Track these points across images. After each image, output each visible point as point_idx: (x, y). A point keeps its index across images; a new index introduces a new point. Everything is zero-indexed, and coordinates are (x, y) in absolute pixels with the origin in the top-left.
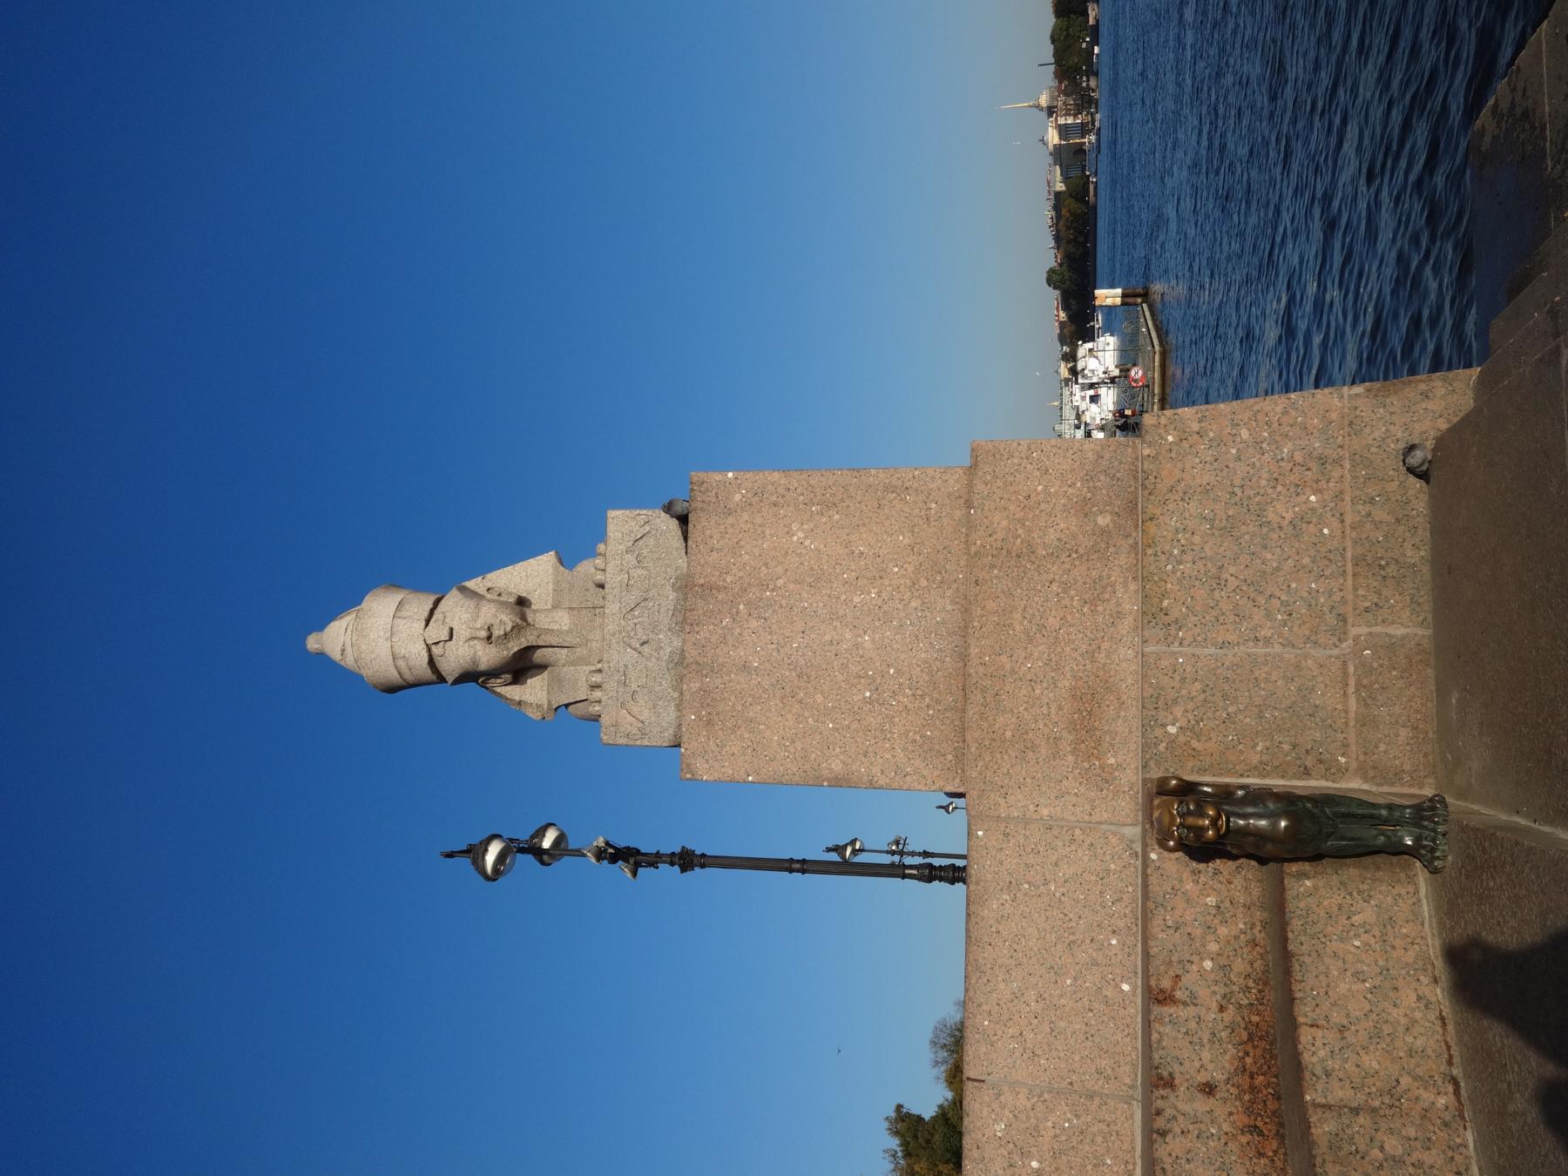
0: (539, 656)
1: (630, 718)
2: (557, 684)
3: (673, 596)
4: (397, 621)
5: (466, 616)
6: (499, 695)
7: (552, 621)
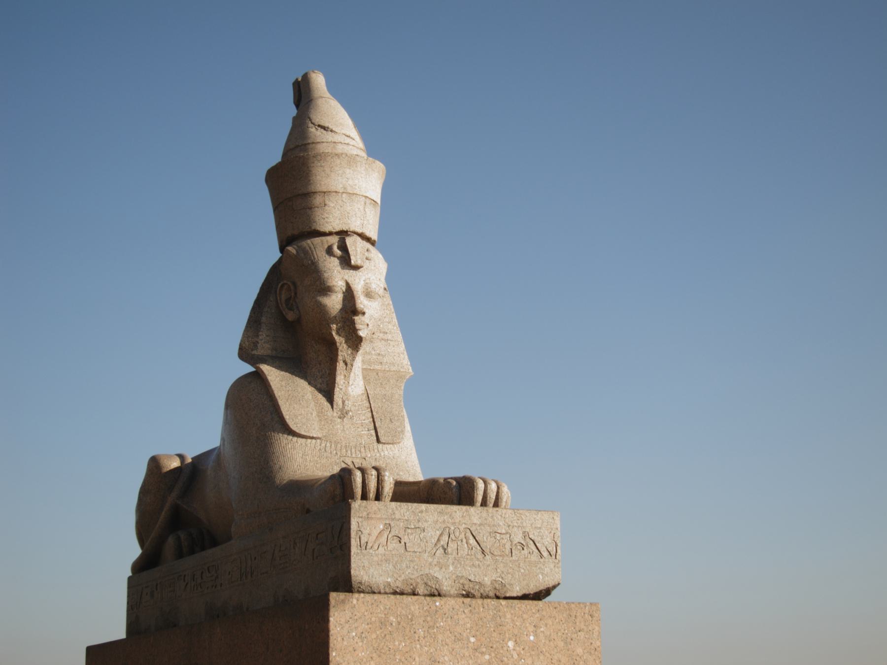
1: (375, 533)
3: (487, 581)
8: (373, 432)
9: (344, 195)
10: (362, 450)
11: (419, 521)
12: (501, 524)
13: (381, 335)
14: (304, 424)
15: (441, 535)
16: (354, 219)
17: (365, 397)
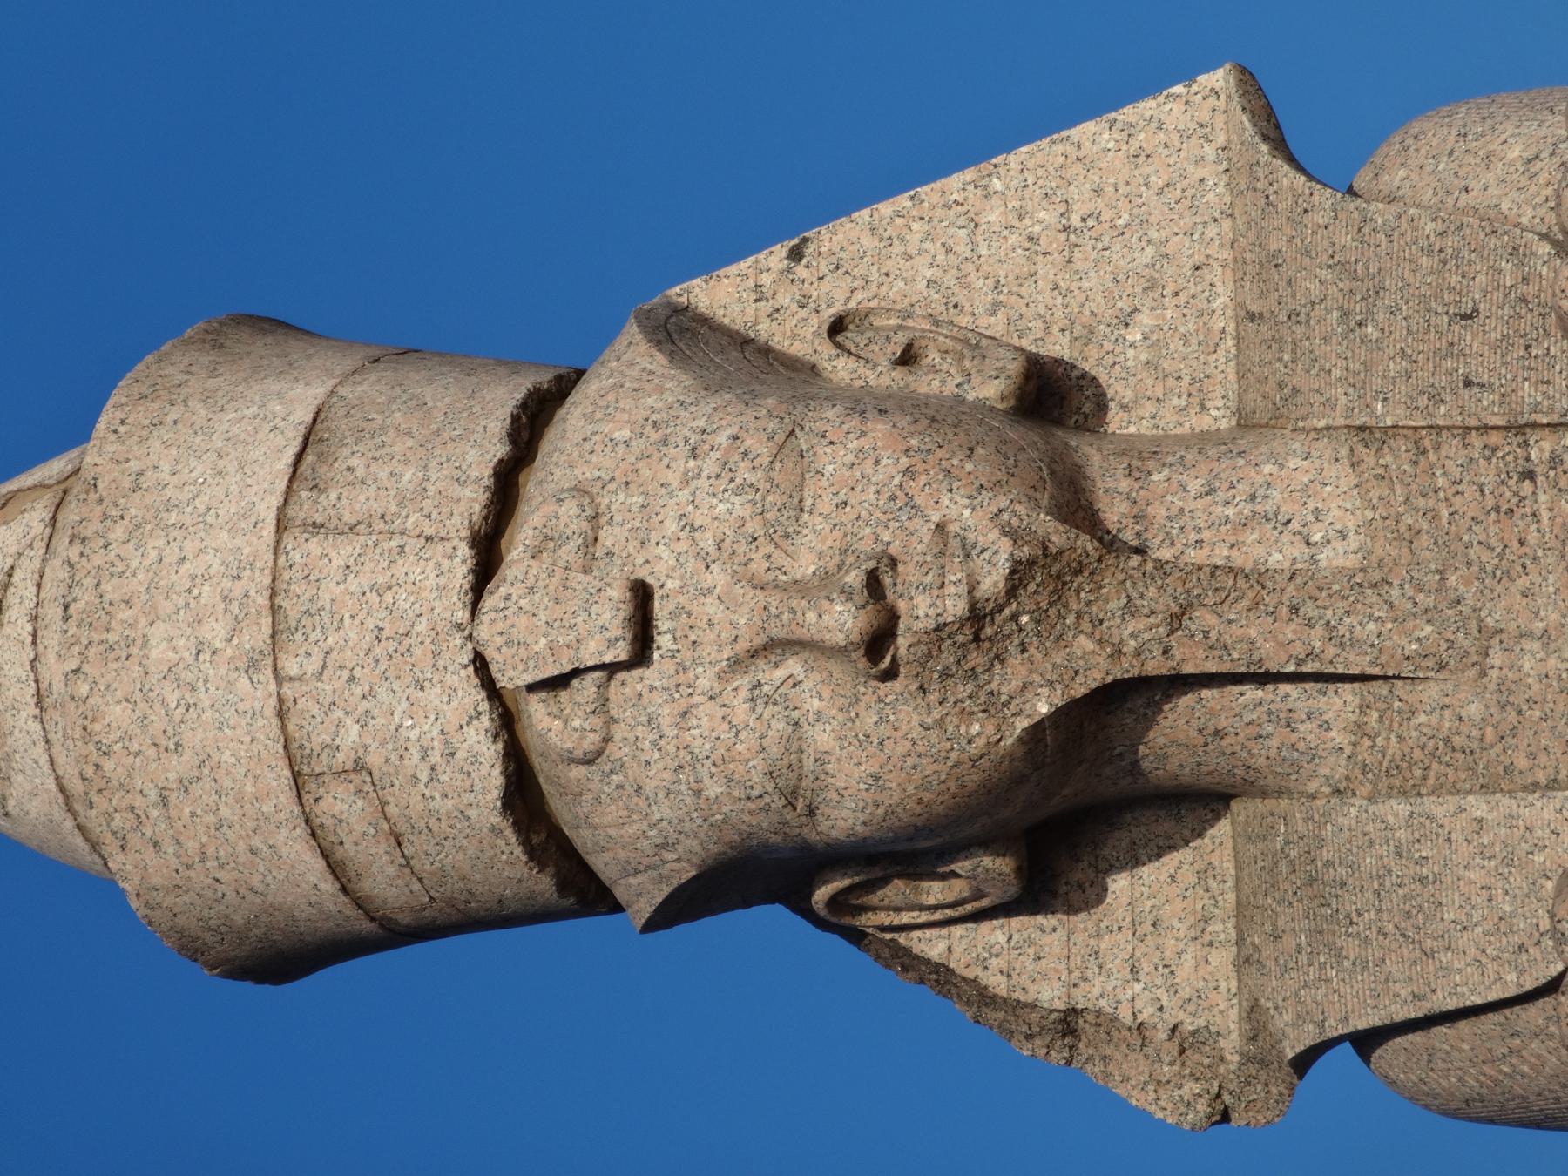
0: (1176, 738)
2: (1292, 902)
4: (302, 549)
5: (722, 510)
6: (940, 977)
7: (1258, 518)
8: (1541, 448)
9: (291, 666)
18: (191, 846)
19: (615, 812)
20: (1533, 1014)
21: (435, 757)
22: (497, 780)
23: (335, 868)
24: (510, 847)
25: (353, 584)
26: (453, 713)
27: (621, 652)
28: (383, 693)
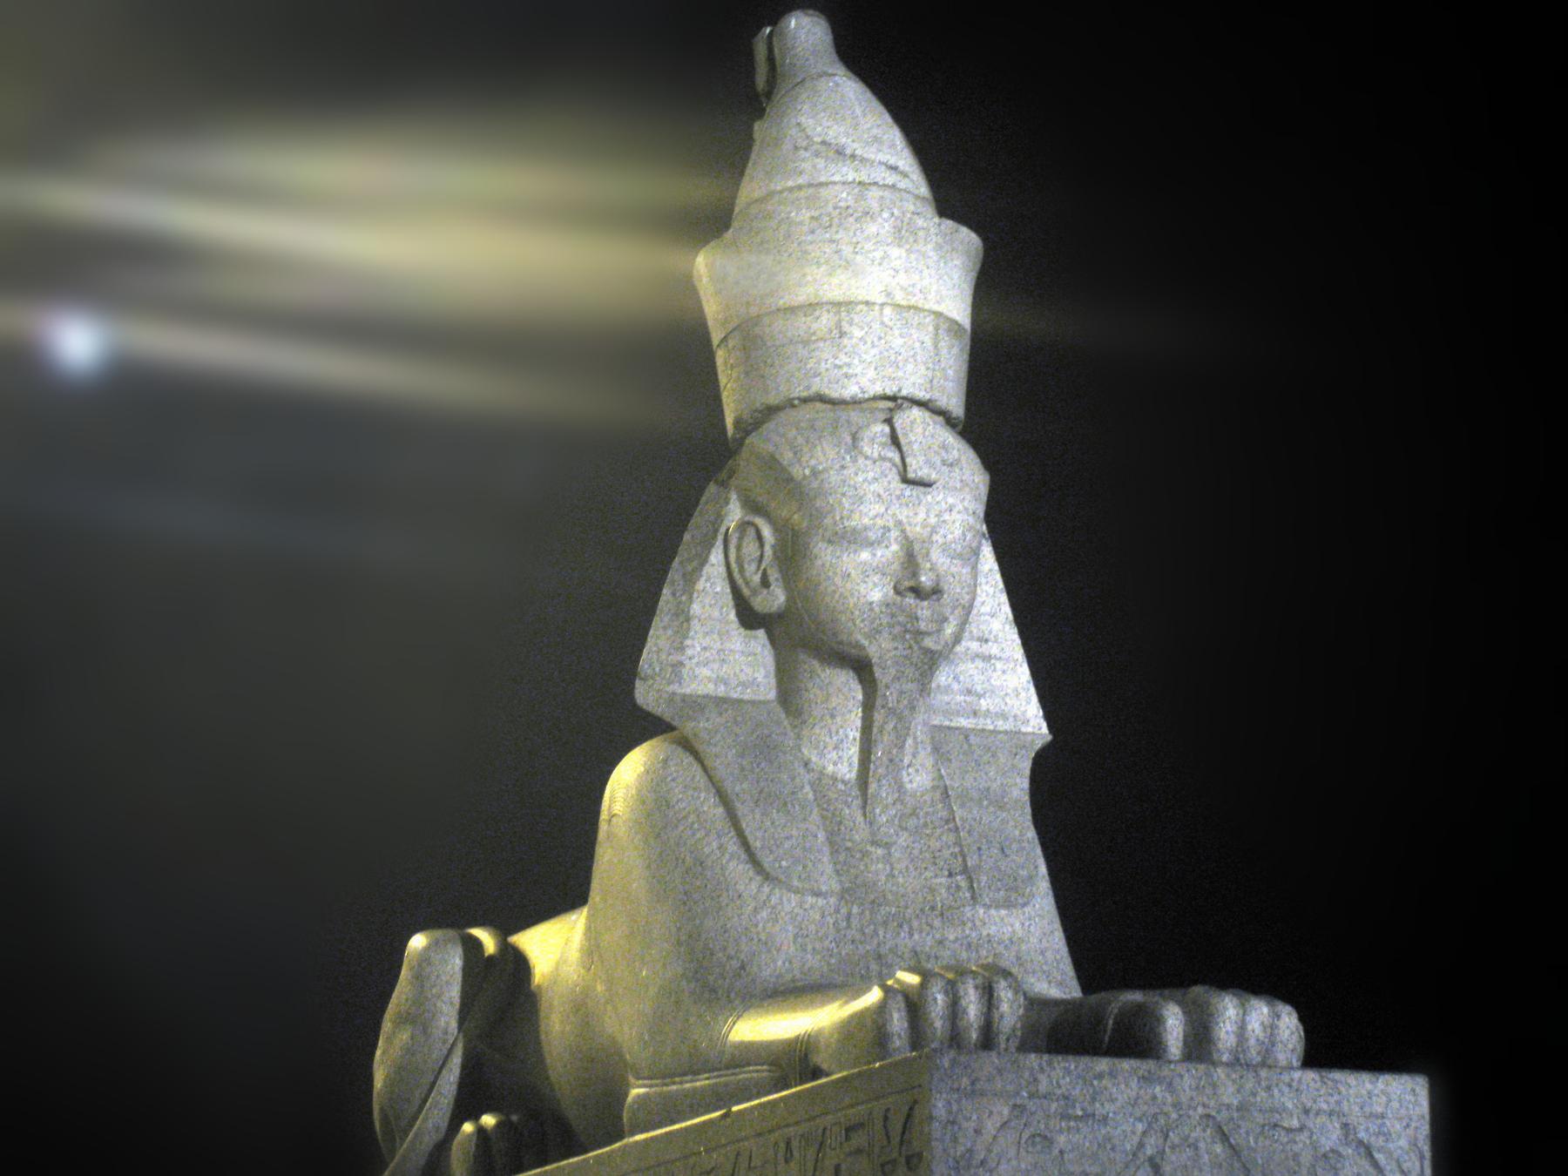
1: (991, 1126)
9: (888, 311)
10: (937, 923)
11: (1094, 1100)
12: (1290, 1105)
13: (974, 646)
14: (797, 861)
15: (1144, 1133)
16: (910, 367)
17: (938, 795)
18: (810, 248)
19: (832, 454)
20: (733, 846)
21: (845, 370)
22: (834, 393)
23: (792, 310)
24: (799, 392)
25: (917, 345)
26: (864, 382)
27: (911, 475)
28: (875, 351)
